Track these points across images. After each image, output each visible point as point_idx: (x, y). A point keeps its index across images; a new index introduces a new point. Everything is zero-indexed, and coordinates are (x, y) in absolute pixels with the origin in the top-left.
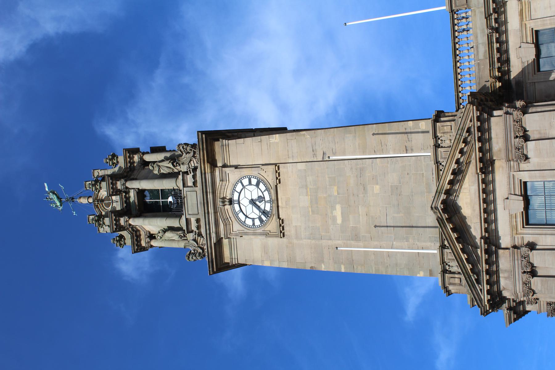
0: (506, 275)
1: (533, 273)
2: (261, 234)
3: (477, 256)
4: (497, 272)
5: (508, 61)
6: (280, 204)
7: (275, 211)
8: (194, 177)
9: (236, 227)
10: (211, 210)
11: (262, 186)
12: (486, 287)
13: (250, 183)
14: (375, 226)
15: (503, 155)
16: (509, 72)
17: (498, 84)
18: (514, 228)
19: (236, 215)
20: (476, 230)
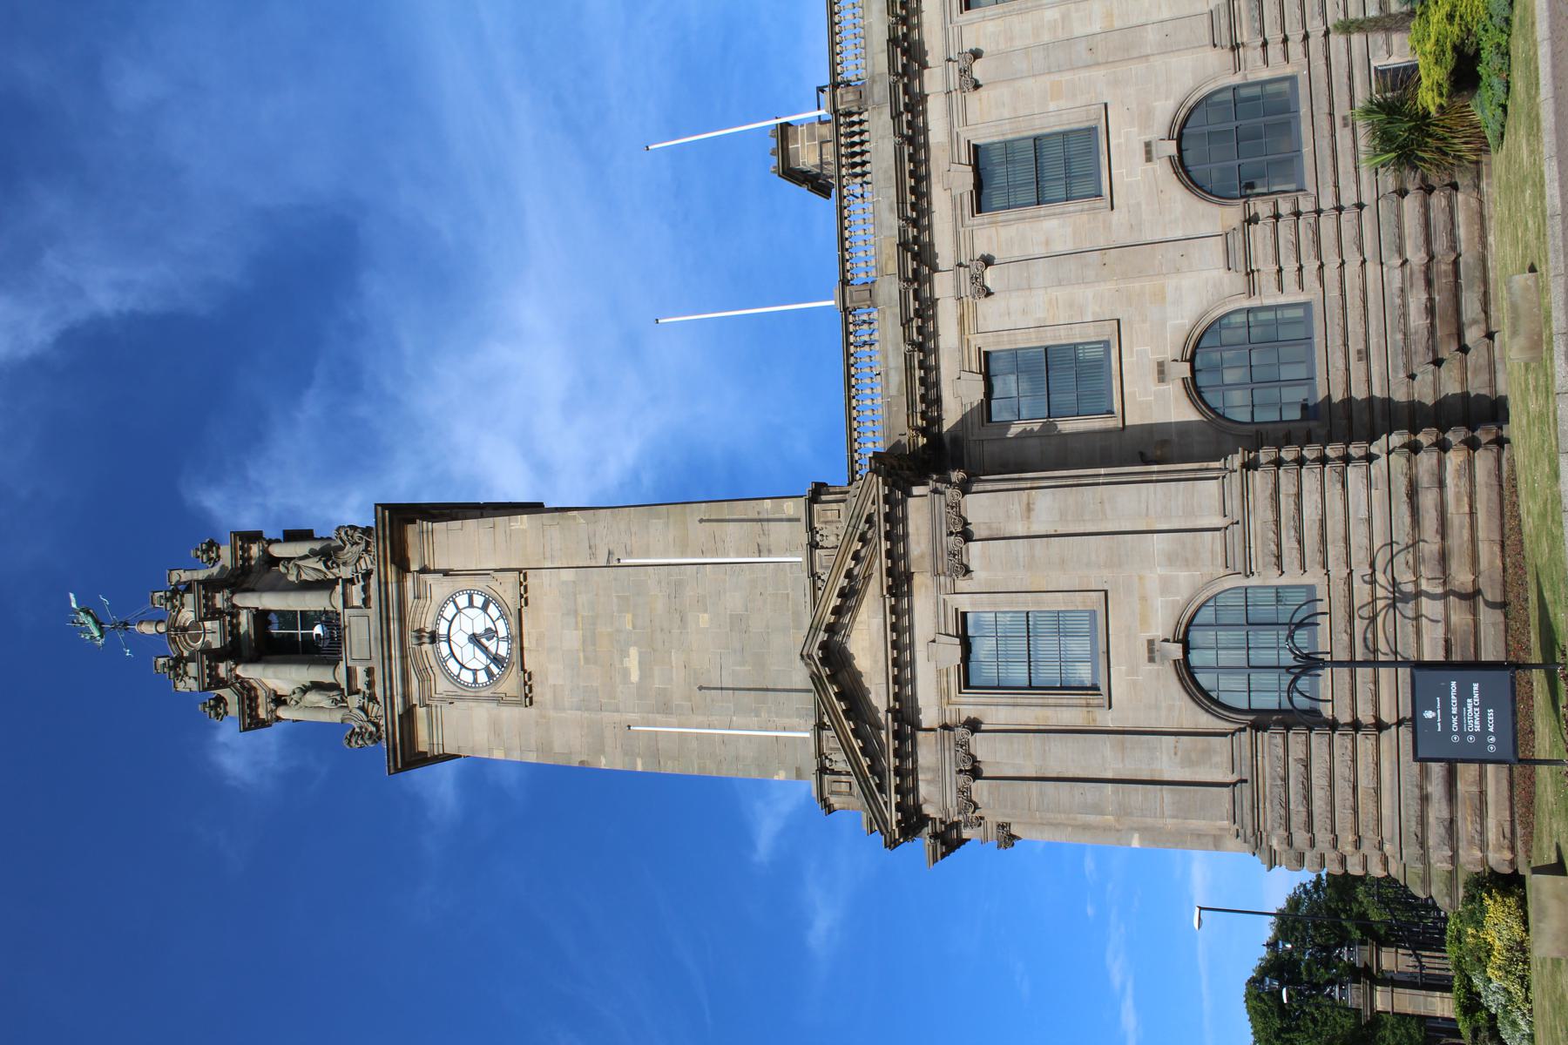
0: (929, 776)
1: (975, 773)
2: (489, 699)
3: (880, 742)
4: (914, 771)
5: (938, 401)
6: (526, 645)
7: (516, 658)
8: (365, 589)
9: (443, 686)
10: (396, 653)
11: (492, 609)
12: (895, 798)
13: (471, 605)
14: (701, 688)
15: (927, 564)
16: (939, 419)
17: (922, 441)
18: (944, 694)
19: (442, 663)
20: (879, 697)
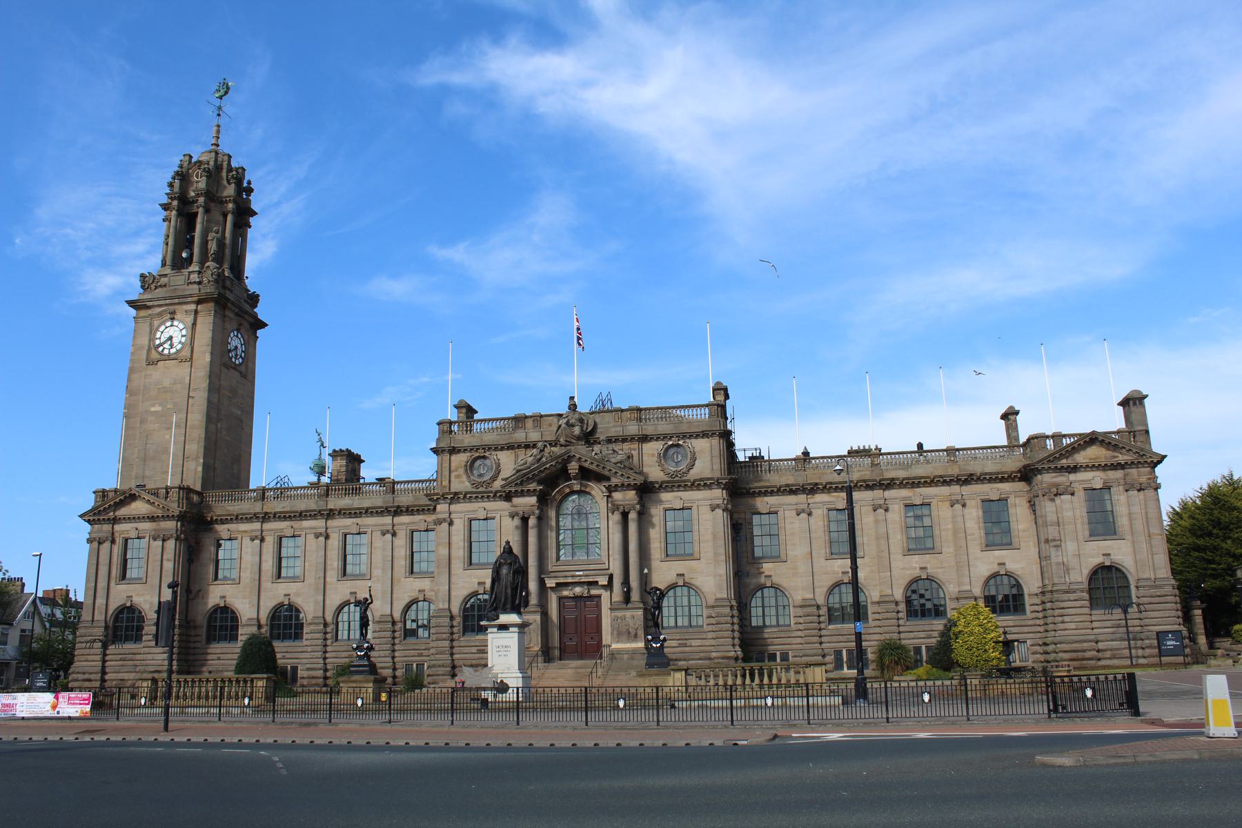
1: (100, 543)
19: (163, 323)
20: (123, 512)
